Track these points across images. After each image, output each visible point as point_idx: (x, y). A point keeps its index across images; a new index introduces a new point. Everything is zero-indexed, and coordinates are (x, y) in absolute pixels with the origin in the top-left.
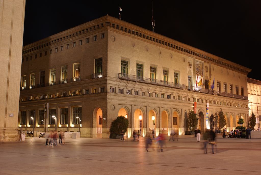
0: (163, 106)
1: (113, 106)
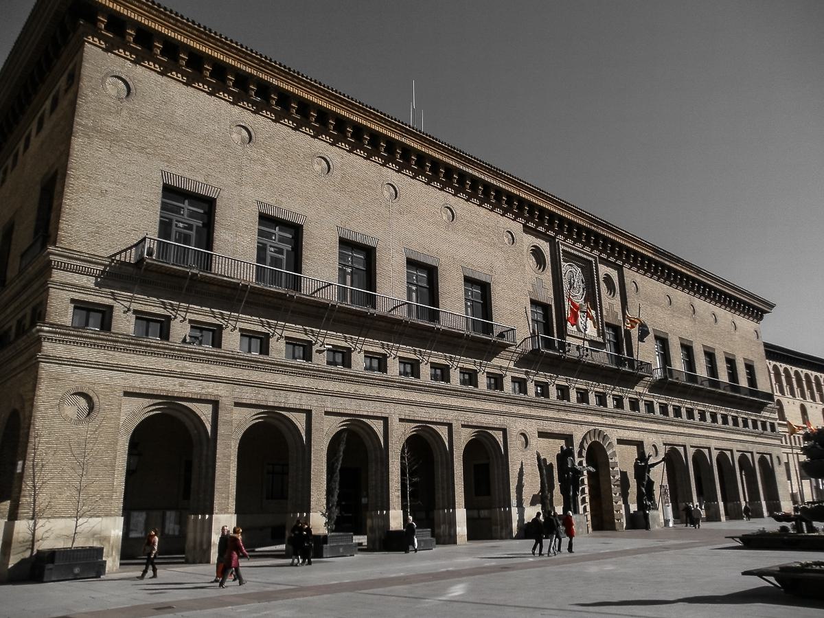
0: (407, 412)
1: (83, 403)
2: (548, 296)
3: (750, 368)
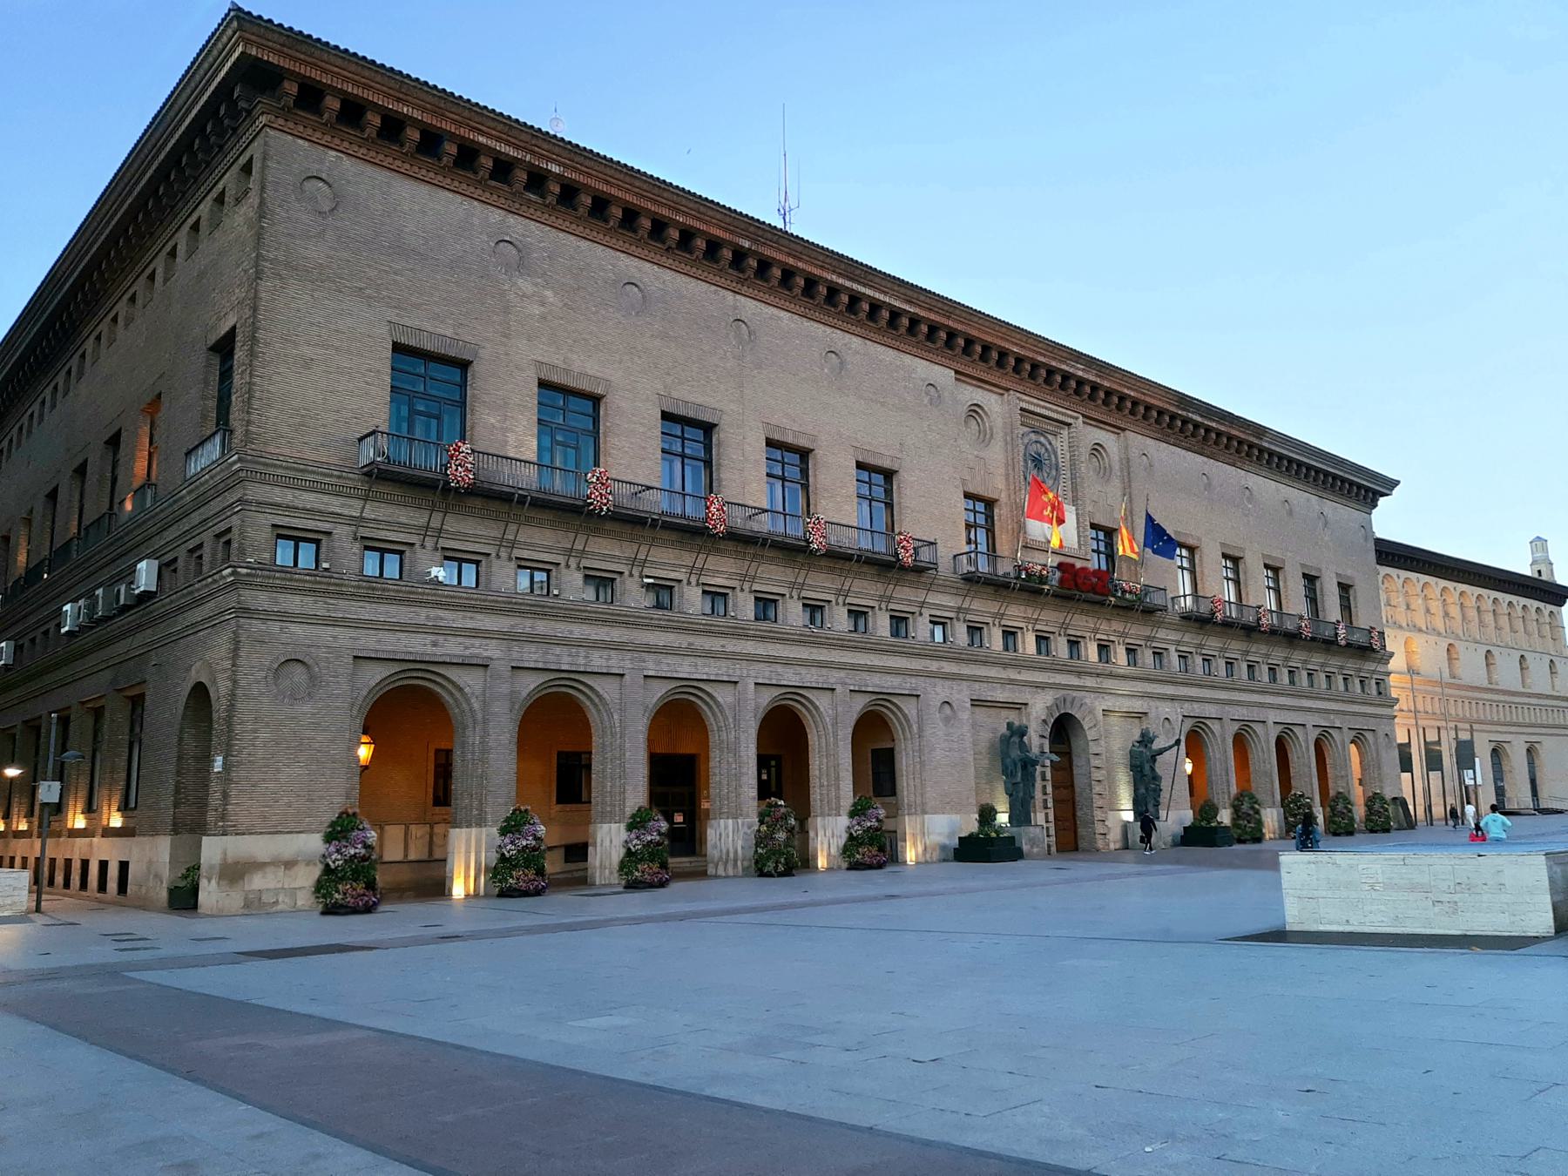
0: (765, 673)
2: (996, 486)
3: (1345, 588)
